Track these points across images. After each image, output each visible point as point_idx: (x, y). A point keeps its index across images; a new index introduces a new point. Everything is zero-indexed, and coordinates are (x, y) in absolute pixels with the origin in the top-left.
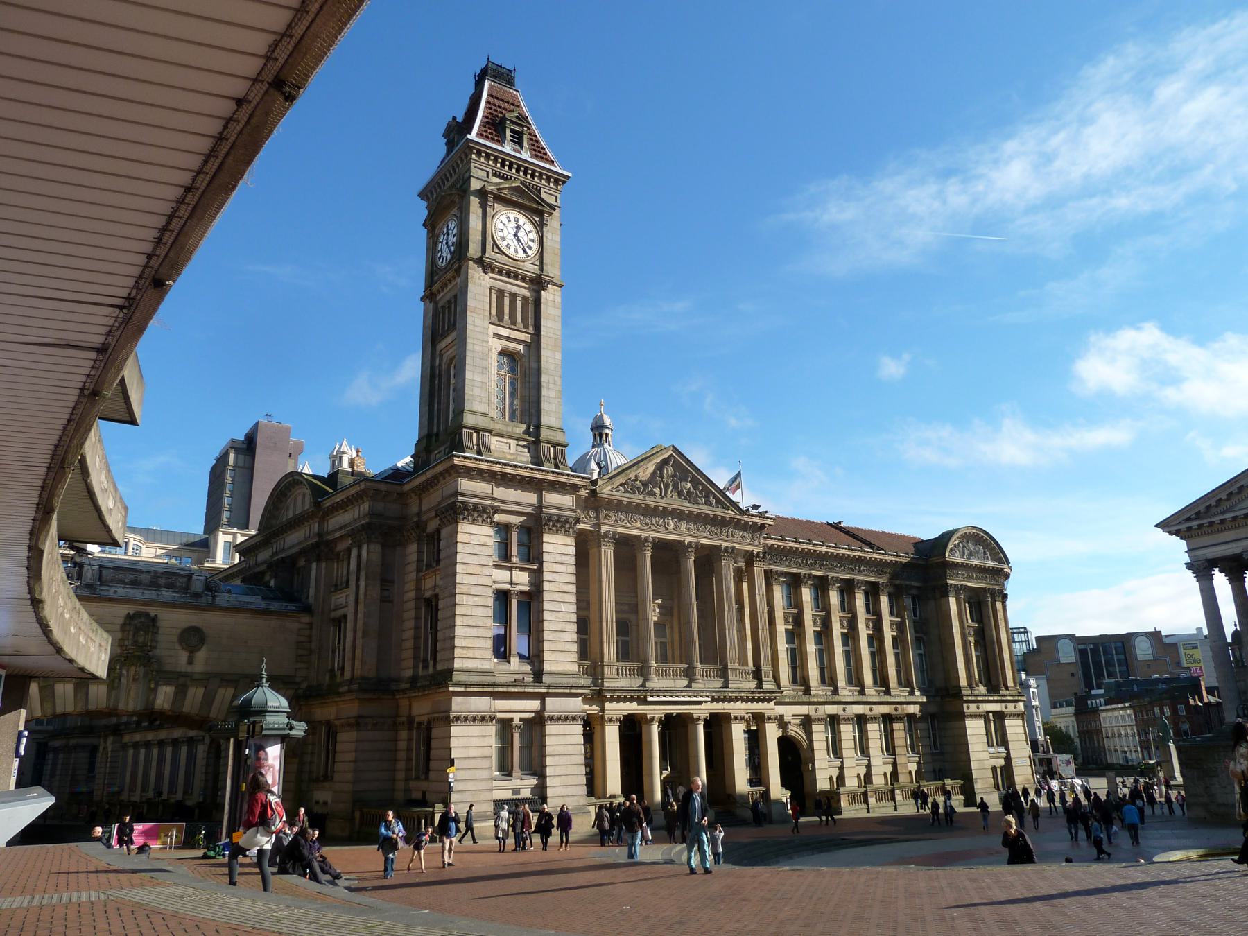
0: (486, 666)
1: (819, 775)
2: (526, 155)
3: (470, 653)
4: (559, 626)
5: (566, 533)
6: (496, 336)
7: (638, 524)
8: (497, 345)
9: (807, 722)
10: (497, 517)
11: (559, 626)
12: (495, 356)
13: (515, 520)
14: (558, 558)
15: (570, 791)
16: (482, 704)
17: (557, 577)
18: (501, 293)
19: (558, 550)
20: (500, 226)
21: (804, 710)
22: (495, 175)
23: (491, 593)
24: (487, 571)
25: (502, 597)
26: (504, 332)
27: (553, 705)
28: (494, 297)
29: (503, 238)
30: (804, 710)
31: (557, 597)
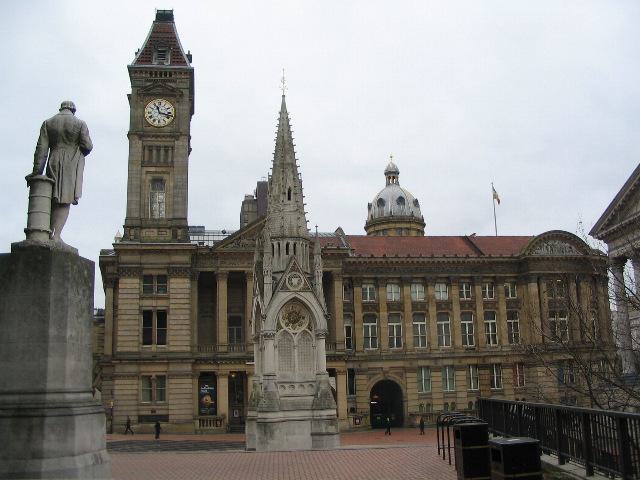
0: (136, 350)
1: (410, 403)
2: (167, 64)
3: (126, 344)
4: (179, 327)
5: (185, 277)
6: (147, 172)
7: (246, 264)
8: (150, 177)
9: (405, 370)
10: (145, 272)
11: (179, 327)
12: (148, 183)
13: (154, 272)
14: (179, 291)
15: (183, 412)
16: (132, 369)
17: (177, 301)
18: (150, 148)
19: (181, 288)
20: (150, 110)
21: (400, 364)
22: (148, 81)
23: (138, 312)
24: (135, 301)
25: (147, 315)
26: (153, 169)
27: (174, 368)
28: (147, 152)
29: (151, 117)
30: (400, 364)
31: (178, 312)
